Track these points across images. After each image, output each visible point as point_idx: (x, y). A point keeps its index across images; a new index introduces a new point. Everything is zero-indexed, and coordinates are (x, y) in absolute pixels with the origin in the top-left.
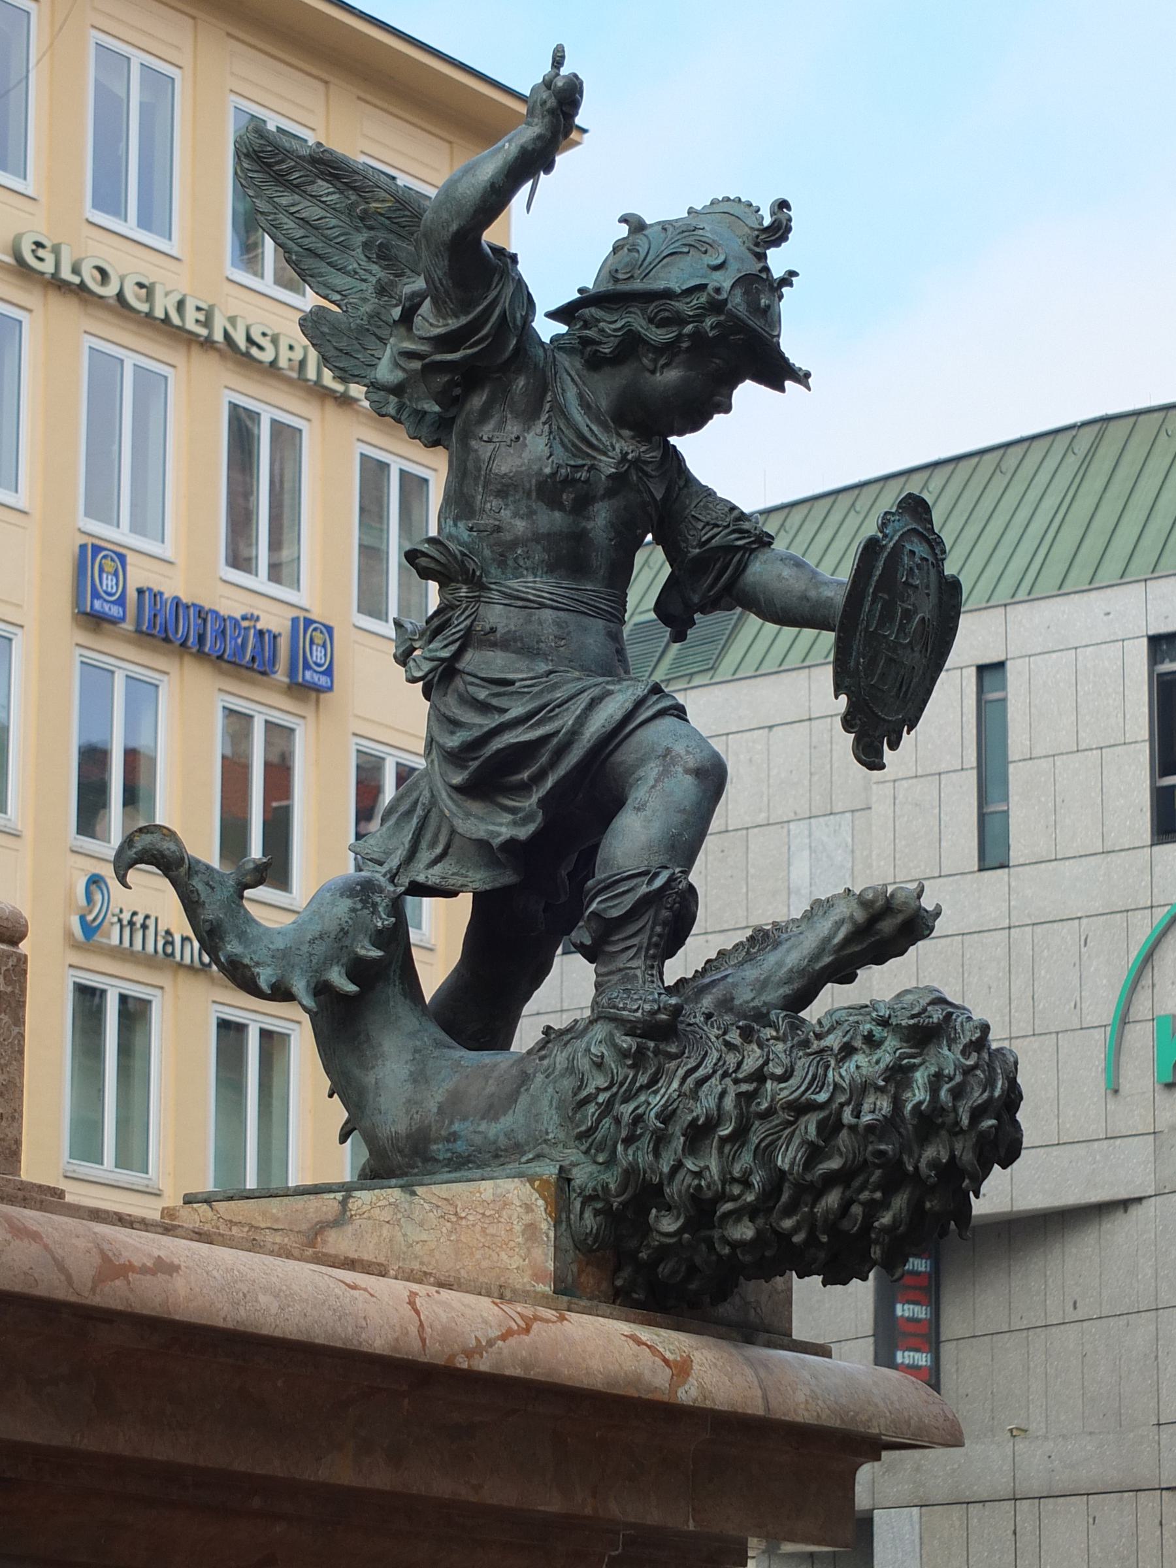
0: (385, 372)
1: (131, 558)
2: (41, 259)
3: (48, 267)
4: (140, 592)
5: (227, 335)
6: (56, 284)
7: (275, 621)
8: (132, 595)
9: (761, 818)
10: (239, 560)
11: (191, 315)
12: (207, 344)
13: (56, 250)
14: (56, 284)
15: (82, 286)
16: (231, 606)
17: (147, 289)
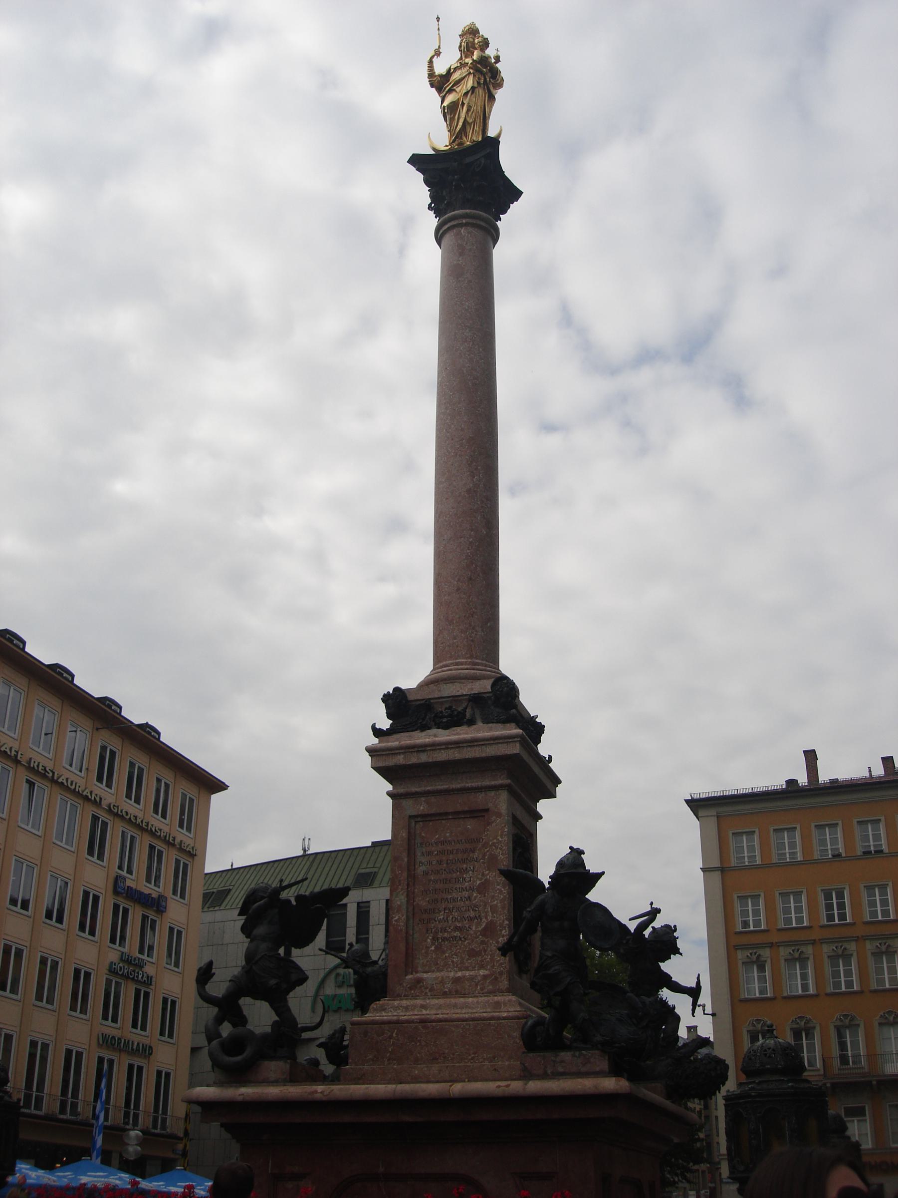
0: (622, 951)
1: (127, 879)
2: (114, 809)
3: (116, 811)
4: (128, 887)
5: (151, 829)
6: (116, 815)
7: (155, 895)
8: (126, 888)
9: (231, 942)
10: (148, 880)
11: (144, 824)
12: (146, 830)
13: (118, 807)
14: (116, 815)
15: (122, 816)
16: (147, 891)
17: (136, 817)
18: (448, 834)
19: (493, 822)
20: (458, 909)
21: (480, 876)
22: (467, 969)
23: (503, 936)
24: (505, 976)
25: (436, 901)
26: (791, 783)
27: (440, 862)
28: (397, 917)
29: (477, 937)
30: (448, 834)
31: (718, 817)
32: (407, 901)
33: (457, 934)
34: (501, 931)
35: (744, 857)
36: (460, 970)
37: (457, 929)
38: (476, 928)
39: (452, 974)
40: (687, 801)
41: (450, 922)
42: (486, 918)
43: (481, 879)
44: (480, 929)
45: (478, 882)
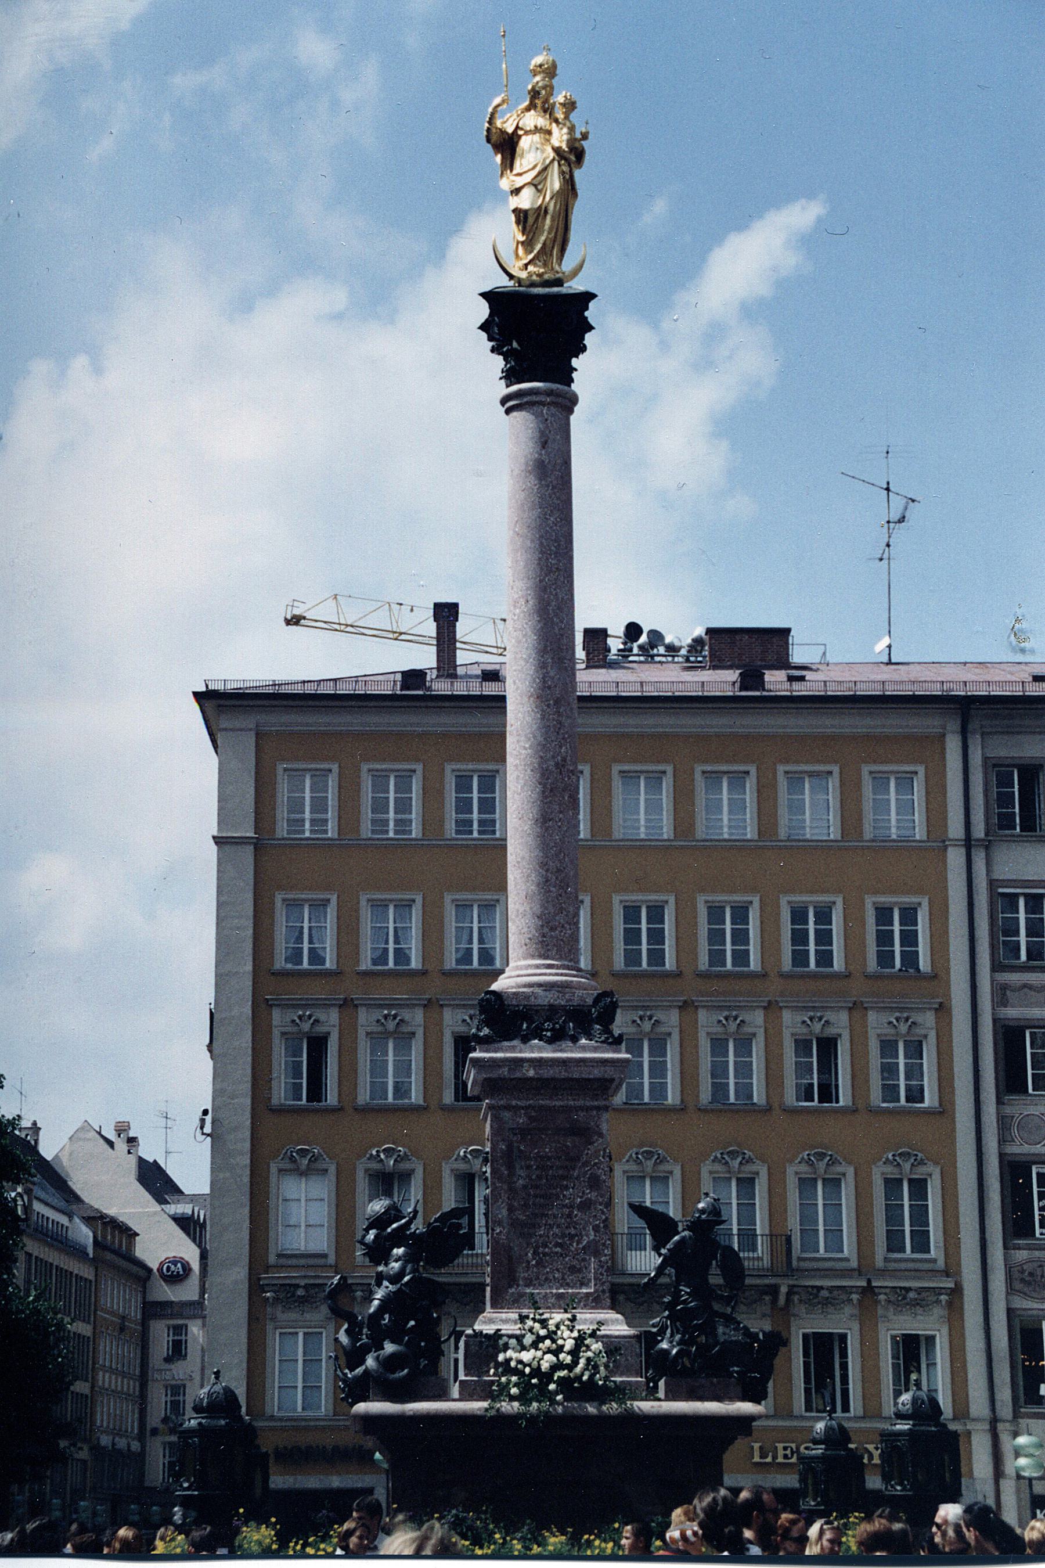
18: (547, 1150)
19: (594, 1142)
20: (558, 1226)
21: (580, 1194)
22: (568, 1285)
23: (606, 1255)
24: (607, 1295)
25: (536, 1215)
26: (413, 677)
27: (539, 1177)
28: (498, 1231)
29: (578, 1254)
30: (547, 1150)
31: (257, 734)
32: (509, 1215)
33: (558, 1249)
34: (603, 1250)
35: (303, 820)
36: (562, 1286)
37: (557, 1245)
38: (577, 1245)
39: (554, 1291)
40: (197, 695)
41: (551, 1238)
42: (587, 1236)
43: (581, 1197)
44: (581, 1246)
45: (579, 1200)
